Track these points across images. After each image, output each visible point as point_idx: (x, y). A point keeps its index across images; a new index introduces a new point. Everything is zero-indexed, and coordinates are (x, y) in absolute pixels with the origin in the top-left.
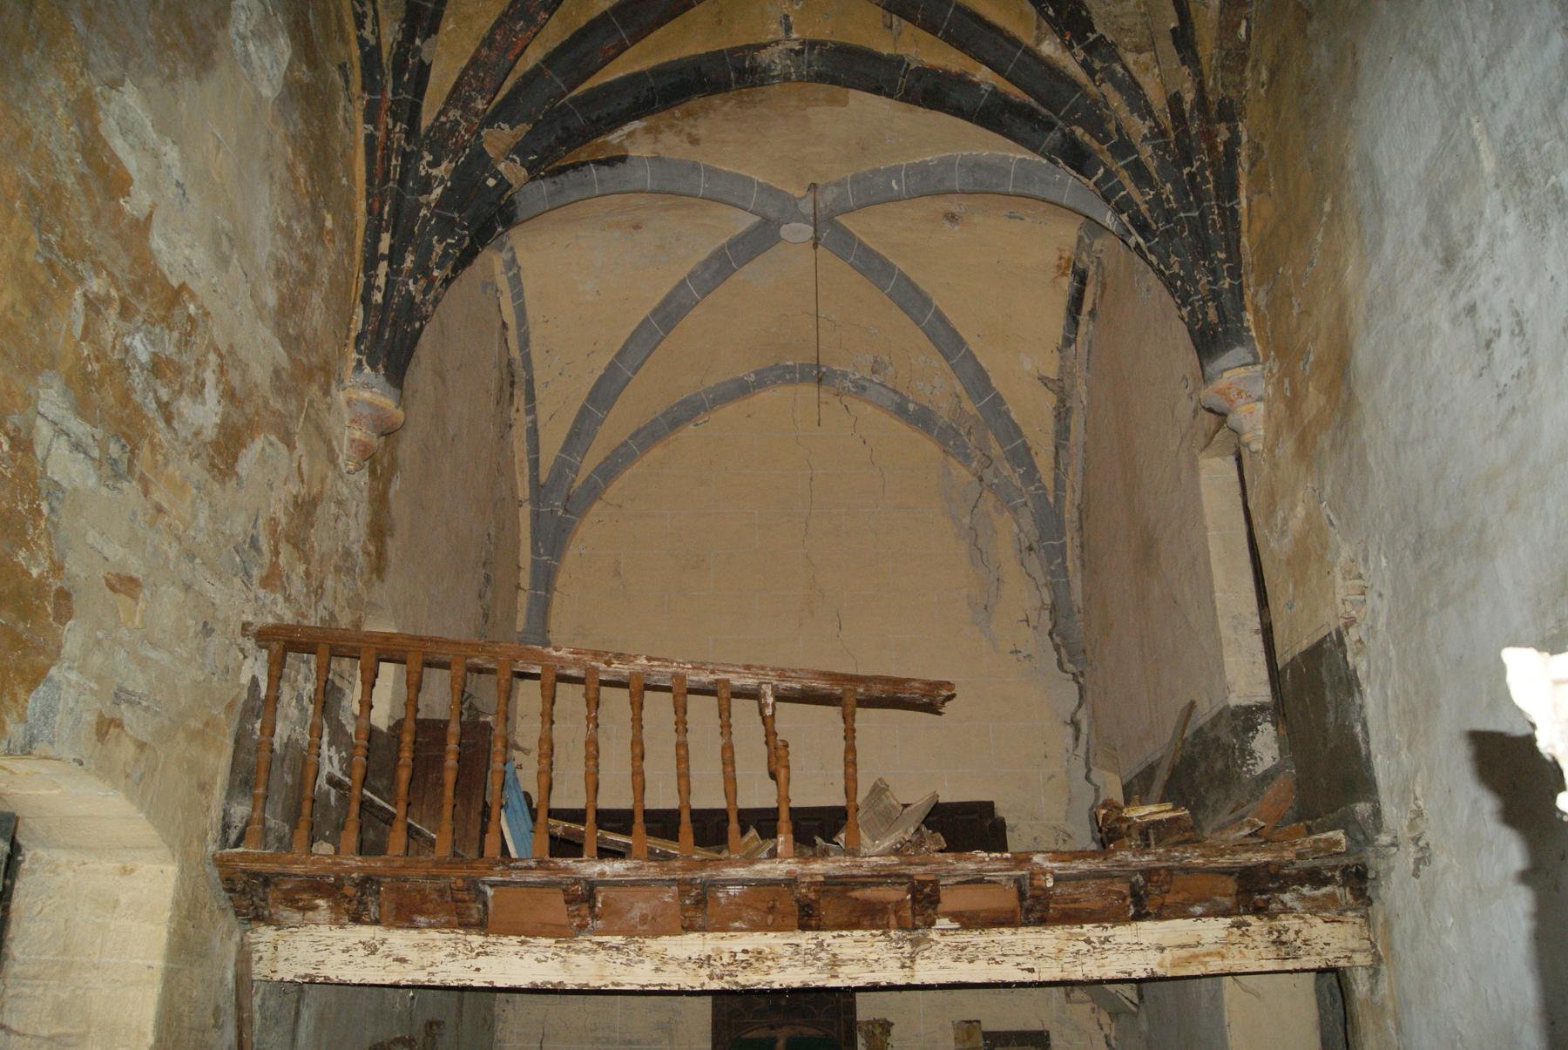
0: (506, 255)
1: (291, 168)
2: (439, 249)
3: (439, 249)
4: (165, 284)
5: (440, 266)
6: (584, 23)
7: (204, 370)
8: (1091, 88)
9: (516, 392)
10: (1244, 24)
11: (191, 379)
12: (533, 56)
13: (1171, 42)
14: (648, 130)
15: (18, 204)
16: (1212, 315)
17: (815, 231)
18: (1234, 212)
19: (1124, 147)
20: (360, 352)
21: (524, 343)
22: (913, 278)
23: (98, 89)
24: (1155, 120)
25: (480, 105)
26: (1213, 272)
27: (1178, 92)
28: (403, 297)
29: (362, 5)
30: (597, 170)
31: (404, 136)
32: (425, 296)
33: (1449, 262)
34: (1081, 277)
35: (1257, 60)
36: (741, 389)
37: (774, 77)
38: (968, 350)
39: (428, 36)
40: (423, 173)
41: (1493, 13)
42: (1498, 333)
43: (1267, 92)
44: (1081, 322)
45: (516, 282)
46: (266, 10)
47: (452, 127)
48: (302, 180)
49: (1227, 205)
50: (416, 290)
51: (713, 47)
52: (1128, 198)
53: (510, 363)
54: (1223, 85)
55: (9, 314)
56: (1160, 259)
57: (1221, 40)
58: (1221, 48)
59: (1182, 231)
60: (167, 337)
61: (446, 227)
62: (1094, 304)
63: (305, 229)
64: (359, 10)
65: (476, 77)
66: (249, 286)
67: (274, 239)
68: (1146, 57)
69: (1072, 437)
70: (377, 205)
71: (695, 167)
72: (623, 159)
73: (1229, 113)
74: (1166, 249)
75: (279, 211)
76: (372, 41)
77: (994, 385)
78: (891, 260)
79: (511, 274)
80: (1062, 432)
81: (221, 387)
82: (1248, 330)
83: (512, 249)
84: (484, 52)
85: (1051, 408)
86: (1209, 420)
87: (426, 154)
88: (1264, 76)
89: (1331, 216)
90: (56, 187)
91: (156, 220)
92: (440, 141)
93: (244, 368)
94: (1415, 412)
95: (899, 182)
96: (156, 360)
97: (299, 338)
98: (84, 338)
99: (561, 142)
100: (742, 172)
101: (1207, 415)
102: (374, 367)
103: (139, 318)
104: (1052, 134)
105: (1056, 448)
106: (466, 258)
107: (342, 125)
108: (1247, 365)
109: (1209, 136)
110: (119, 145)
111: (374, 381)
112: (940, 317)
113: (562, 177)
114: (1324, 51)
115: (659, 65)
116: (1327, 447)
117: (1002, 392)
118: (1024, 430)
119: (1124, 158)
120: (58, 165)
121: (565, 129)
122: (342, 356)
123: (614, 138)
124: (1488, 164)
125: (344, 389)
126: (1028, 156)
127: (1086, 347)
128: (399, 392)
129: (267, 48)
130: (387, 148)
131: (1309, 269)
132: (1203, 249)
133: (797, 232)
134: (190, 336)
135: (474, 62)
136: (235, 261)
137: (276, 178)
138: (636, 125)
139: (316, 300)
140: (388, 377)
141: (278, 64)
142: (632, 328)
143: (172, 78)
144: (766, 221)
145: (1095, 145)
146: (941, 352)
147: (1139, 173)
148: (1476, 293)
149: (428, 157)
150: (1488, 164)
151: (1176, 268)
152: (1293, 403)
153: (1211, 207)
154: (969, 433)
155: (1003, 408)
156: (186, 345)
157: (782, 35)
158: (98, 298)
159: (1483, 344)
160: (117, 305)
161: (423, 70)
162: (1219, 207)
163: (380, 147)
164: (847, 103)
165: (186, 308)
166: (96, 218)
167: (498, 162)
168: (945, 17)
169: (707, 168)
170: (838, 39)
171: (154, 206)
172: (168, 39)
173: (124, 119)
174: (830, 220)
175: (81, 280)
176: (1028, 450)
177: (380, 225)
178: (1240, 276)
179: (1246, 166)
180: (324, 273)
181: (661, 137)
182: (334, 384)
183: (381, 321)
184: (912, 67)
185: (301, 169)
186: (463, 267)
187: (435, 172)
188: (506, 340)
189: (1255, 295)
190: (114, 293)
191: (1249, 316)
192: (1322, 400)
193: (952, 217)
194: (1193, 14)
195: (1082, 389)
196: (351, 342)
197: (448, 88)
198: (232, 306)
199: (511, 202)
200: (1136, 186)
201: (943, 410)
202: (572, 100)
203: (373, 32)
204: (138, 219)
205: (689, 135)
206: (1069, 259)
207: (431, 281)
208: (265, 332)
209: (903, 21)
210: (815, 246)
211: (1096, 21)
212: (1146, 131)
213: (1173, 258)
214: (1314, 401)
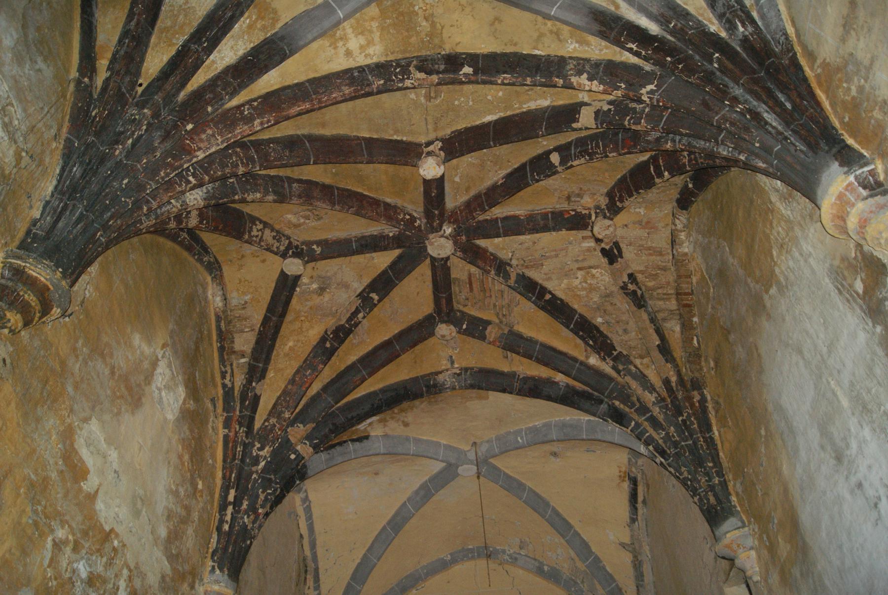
0: (302, 495)
1: (180, 457)
2: (262, 497)
3: (262, 497)
4: (102, 529)
5: (262, 507)
6: (343, 369)
7: (120, 580)
8: (620, 379)
9: (308, 576)
10: (695, 338)
11: (111, 586)
12: (316, 387)
13: (658, 352)
14: (380, 421)
15: (22, 490)
16: (712, 500)
17: (478, 469)
18: (712, 439)
19: (643, 409)
20: (214, 561)
21: (313, 546)
22: (537, 491)
23: (76, 424)
24: (657, 392)
25: (287, 415)
26: (707, 474)
27: (667, 377)
28: (241, 526)
29: (225, 367)
30: (352, 445)
31: (244, 434)
32: (253, 524)
33: (839, 458)
34: (634, 482)
35: (707, 356)
36: (443, 566)
37: (446, 388)
38: (575, 530)
39: (260, 380)
40: (255, 454)
41: (824, 323)
42: (879, 498)
43: (716, 372)
44: (639, 508)
45: (308, 510)
46: (173, 374)
47: (271, 428)
48: (186, 464)
49: (708, 436)
50: (249, 521)
51: (413, 375)
52: (650, 436)
53: (304, 559)
54: (691, 371)
55: (7, 556)
56: (676, 470)
57: (685, 348)
58: (686, 352)
59: (685, 453)
60: (99, 561)
61: (267, 483)
62: (644, 497)
63: (186, 490)
64: (223, 369)
65: (285, 400)
66: (151, 526)
67: (167, 498)
68: (646, 361)
69: (645, 579)
70: (228, 474)
71: (407, 439)
72: (367, 437)
73: (697, 385)
74: (678, 464)
75: (172, 482)
76: (230, 385)
77: (593, 551)
78: (523, 481)
79: (305, 506)
80: (639, 576)
81: (129, 590)
82: (735, 507)
83: (306, 491)
84: (290, 387)
85: (630, 562)
86: (725, 564)
87: (256, 443)
88: (712, 364)
89: (766, 436)
90: (46, 479)
91: (100, 494)
92: (264, 437)
93: (143, 576)
94: (845, 550)
95: (522, 438)
96: (91, 576)
97: (178, 555)
98: (49, 566)
99: (331, 431)
100: (434, 439)
101: (723, 561)
102: (221, 570)
103: (84, 551)
104: (602, 406)
105: (637, 587)
106: (278, 500)
107: (211, 431)
108: (739, 528)
109: (689, 399)
110: (85, 453)
111: (221, 579)
112: (556, 513)
113: (333, 450)
114: (741, 349)
115: (384, 387)
116: (798, 575)
117: (598, 554)
118: (616, 577)
119: (644, 415)
120: (48, 467)
121: (334, 424)
122: (203, 564)
123: (362, 426)
124: (845, 403)
125: (203, 585)
126: (592, 418)
127: (644, 523)
128: (235, 585)
129: (172, 394)
130: (235, 442)
131: (761, 469)
132: (699, 462)
133: (468, 470)
134: (113, 559)
135: (285, 392)
136: (144, 512)
137: (172, 463)
138: (374, 418)
139: (190, 531)
140: (230, 576)
141: (178, 402)
142: (376, 533)
143: (119, 413)
144: (450, 465)
145: (627, 409)
146: (559, 533)
147: (654, 421)
148: (860, 476)
149: (258, 445)
150: (845, 403)
151: (686, 474)
152: (772, 549)
153: (698, 438)
154: (583, 582)
155: (601, 565)
156: (110, 565)
157: (449, 366)
158: (61, 541)
159: (873, 505)
160: (71, 545)
161: (257, 399)
162: (703, 438)
163: (231, 441)
164: (488, 398)
165: (112, 542)
166: (66, 495)
167: (296, 445)
168: (535, 350)
169: (415, 439)
170: (479, 366)
171: (100, 485)
172: (118, 394)
173: (89, 438)
174: (486, 461)
175: (52, 531)
176: (620, 590)
177: (229, 485)
178: (723, 475)
179: (713, 413)
180: (195, 516)
181: (387, 424)
182: (197, 581)
183: (227, 541)
184: (521, 377)
185: (186, 457)
186: (276, 506)
187: (261, 453)
188: (302, 545)
189: (734, 486)
190: (70, 537)
191: (734, 498)
192: (789, 547)
193: (555, 454)
194: (667, 336)
195: (646, 549)
196: (209, 555)
197: (270, 406)
198: (140, 540)
199: (304, 466)
200: (654, 430)
201: (565, 568)
202: (338, 409)
203: (230, 381)
204: (90, 494)
205: (403, 422)
206: (625, 472)
207: (257, 515)
208: (158, 553)
209: (514, 355)
210: (478, 477)
211: (616, 345)
212: (654, 400)
213: (683, 469)
214: (784, 549)
